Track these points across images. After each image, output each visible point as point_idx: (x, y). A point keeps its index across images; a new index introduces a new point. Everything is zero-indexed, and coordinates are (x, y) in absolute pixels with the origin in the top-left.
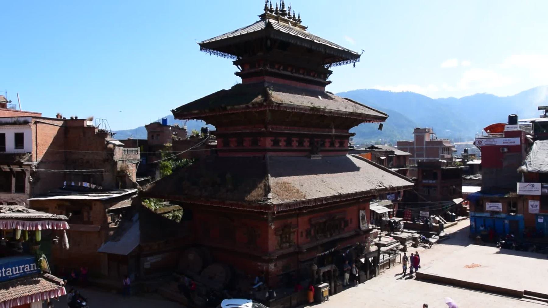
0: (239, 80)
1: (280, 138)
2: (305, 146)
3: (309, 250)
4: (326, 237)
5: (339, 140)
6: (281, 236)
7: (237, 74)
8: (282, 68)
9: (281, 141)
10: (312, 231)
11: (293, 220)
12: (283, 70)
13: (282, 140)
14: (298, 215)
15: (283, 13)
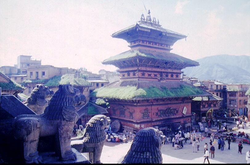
0: (130, 49)
1: (145, 73)
2: (148, 74)
3: (156, 121)
4: (166, 116)
5: (176, 75)
6: (143, 113)
7: (129, 46)
8: (148, 43)
9: (145, 74)
10: (159, 113)
11: (149, 108)
12: (149, 44)
13: (146, 74)
14: (151, 105)
15: (150, 20)
